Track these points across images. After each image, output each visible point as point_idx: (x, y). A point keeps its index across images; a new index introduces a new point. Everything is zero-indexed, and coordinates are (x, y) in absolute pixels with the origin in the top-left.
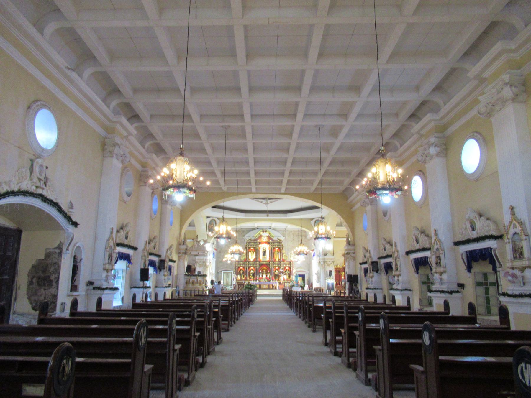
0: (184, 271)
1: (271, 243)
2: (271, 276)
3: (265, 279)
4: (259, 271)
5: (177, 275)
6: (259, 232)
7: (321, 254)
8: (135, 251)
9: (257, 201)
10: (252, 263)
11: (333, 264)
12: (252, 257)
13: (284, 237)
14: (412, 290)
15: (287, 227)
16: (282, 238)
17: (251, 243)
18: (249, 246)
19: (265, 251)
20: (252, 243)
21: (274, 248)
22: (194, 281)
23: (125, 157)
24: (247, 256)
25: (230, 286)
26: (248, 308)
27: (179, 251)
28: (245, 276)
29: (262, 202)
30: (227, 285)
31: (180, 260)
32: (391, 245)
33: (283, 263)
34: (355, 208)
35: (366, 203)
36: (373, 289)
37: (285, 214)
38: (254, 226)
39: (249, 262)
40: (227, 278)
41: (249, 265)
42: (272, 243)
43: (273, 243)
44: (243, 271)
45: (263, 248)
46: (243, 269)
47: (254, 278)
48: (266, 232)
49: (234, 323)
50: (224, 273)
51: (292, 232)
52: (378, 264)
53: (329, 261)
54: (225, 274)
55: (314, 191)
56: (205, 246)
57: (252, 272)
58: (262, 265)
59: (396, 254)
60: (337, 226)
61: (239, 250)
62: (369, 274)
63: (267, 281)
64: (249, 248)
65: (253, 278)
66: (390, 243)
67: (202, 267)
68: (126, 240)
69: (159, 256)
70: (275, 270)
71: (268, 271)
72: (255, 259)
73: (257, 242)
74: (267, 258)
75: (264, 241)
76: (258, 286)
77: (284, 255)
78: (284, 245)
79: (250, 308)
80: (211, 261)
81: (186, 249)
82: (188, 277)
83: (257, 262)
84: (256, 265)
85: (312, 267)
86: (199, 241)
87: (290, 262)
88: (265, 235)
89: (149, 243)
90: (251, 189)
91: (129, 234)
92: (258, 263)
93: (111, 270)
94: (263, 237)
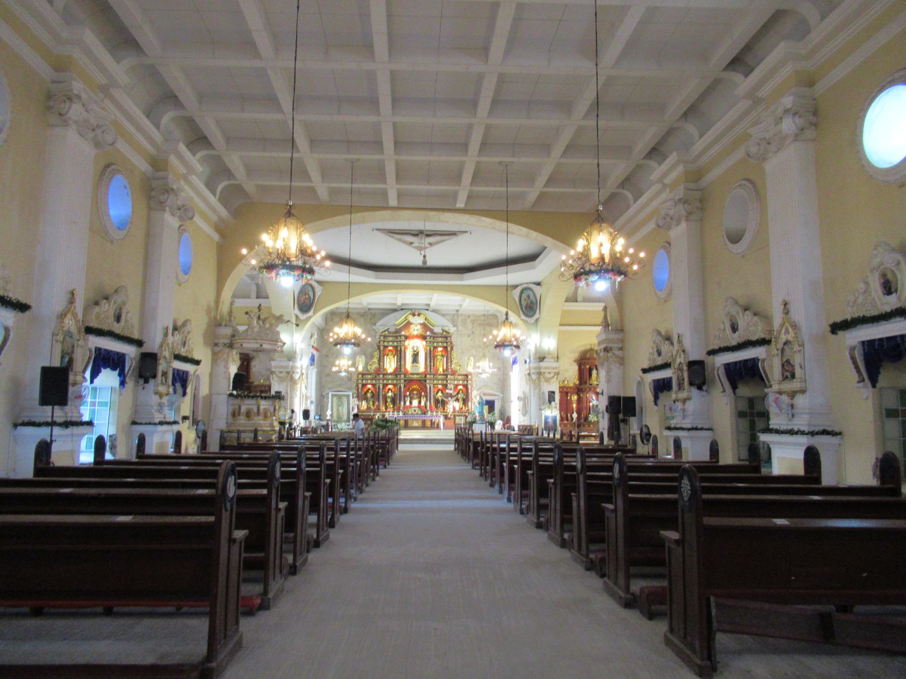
0: (226, 386)
1: (428, 338)
2: (428, 403)
3: (417, 409)
4: (405, 393)
5: (210, 395)
6: (405, 315)
7: (532, 358)
8: (20, 314)
9: (400, 240)
10: (390, 376)
11: (557, 378)
12: (390, 365)
14: (840, 434)
15: (461, 306)
16: (452, 330)
17: (390, 336)
18: (386, 343)
19: (418, 353)
21: (435, 348)
22: (252, 409)
24: (382, 364)
25: (345, 421)
26: (374, 480)
27: (216, 342)
28: (377, 403)
29: (412, 243)
30: (340, 420)
31: (219, 361)
33: (453, 377)
35: (672, 219)
36: (689, 429)
37: (459, 275)
39: (384, 375)
40: (339, 406)
41: (385, 382)
42: (431, 337)
43: (434, 338)
44: (372, 392)
45: (413, 348)
46: (372, 389)
47: (394, 406)
48: (419, 315)
50: (332, 395)
51: (471, 318)
52: (704, 368)
53: (550, 373)
54: (335, 399)
55: (534, 205)
57: (390, 394)
58: (409, 382)
59: (787, 332)
60: (566, 301)
61: (355, 336)
62: (676, 393)
63: (420, 412)
64: (386, 347)
65: (392, 406)
67: (285, 384)
69: (139, 343)
70: (436, 390)
71: (423, 394)
72: (396, 370)
73: (400, 336)
74: (421, 367)
75: (415, 333)
76: (402, 423)
77: (454, 362)
78: (454, 343)
79: (377, 478)
80: (304, 371)
81: (233, 336)
82: (238, 401)
83: (400, 374)
84: (398, 382)
85: (510, 386)
88: (417, 321)
90: (384, 194)
92: (402, 376)
94: (412, 326)
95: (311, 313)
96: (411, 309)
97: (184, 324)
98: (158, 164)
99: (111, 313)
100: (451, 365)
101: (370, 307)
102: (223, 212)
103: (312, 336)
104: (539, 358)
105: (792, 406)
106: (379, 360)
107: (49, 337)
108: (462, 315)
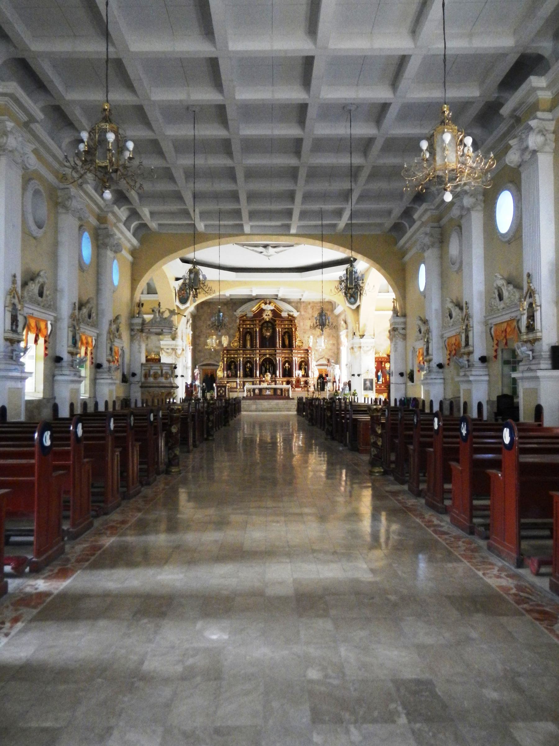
1: (277, 321)
9: (253, 250)
13: (298, 312)
15: (302, 295)
16: (295, 314)
20: (249, 321)
23: (28, 157)
27: (132, 328)
29: (261, 252)
32: (461, 309)
34: (407, 258)
38: (251, 295)
43: (282, 321)
48: (270, 303)
49: (219, 429)
51: (311, 305)
53: (367, 347)
56: (172, 319)
66: (459, 306)
68: (39, 298)
77: (297, 340)
78: (297, 325)
83: (256, 350)
86: (163, 312)
87: (307, 350)
89: (80, 309)
91: (45, 289)
93: (19, 341)
95: (188, 304)
96: (263, 299)
97: (117, 318)
98: (102, 219)
99: (87, 314)
100: (295, 342)
101: (232, 297)
102: (135, 242)
103: (188, 322)
104: (360, 336)
105: (468, 361)
106: (239, 340)
107: (66, 328)
108: (304, 302)
